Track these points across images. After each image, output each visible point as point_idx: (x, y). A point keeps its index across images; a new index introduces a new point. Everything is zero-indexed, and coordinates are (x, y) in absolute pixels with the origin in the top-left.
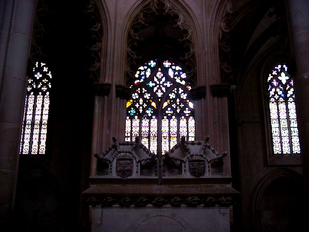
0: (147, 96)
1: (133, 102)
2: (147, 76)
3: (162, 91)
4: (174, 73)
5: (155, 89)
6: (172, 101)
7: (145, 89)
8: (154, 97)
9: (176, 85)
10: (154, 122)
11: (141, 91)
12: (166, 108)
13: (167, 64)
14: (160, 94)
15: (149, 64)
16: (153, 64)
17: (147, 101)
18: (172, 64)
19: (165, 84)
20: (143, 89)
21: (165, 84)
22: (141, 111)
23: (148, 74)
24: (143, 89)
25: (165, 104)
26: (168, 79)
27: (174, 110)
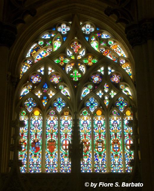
0: (56, 80)
1: (33, 88)
2: (55, 49)
3: (80, 72)
4: (100, 44)
5: (69, 68)
6: (96, 87)
7: (52, 69)
8: (66, 79)
9: (103, 61)
10: (67, 120)
11: (46, 71)
12: (87, 98)
13: (88, 28)
14: (76, 76)
15: (59, 29)
16: (64, 29)
17: (56, 87)
18: (95, 30)
19: (85, 61)
20: (50, 69)
21: (85, 61)
22: (45, 103)
23: (57, 45)
24: (50, 69)
25: (86, 91)
26: (90, 51)
27: (101, 101)
